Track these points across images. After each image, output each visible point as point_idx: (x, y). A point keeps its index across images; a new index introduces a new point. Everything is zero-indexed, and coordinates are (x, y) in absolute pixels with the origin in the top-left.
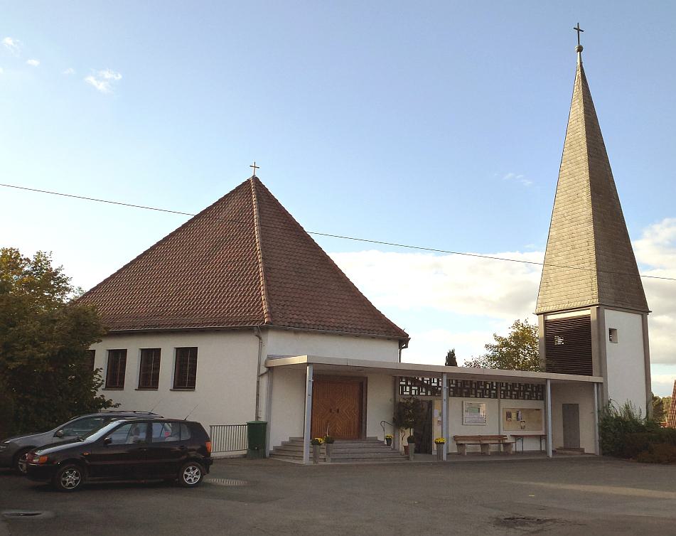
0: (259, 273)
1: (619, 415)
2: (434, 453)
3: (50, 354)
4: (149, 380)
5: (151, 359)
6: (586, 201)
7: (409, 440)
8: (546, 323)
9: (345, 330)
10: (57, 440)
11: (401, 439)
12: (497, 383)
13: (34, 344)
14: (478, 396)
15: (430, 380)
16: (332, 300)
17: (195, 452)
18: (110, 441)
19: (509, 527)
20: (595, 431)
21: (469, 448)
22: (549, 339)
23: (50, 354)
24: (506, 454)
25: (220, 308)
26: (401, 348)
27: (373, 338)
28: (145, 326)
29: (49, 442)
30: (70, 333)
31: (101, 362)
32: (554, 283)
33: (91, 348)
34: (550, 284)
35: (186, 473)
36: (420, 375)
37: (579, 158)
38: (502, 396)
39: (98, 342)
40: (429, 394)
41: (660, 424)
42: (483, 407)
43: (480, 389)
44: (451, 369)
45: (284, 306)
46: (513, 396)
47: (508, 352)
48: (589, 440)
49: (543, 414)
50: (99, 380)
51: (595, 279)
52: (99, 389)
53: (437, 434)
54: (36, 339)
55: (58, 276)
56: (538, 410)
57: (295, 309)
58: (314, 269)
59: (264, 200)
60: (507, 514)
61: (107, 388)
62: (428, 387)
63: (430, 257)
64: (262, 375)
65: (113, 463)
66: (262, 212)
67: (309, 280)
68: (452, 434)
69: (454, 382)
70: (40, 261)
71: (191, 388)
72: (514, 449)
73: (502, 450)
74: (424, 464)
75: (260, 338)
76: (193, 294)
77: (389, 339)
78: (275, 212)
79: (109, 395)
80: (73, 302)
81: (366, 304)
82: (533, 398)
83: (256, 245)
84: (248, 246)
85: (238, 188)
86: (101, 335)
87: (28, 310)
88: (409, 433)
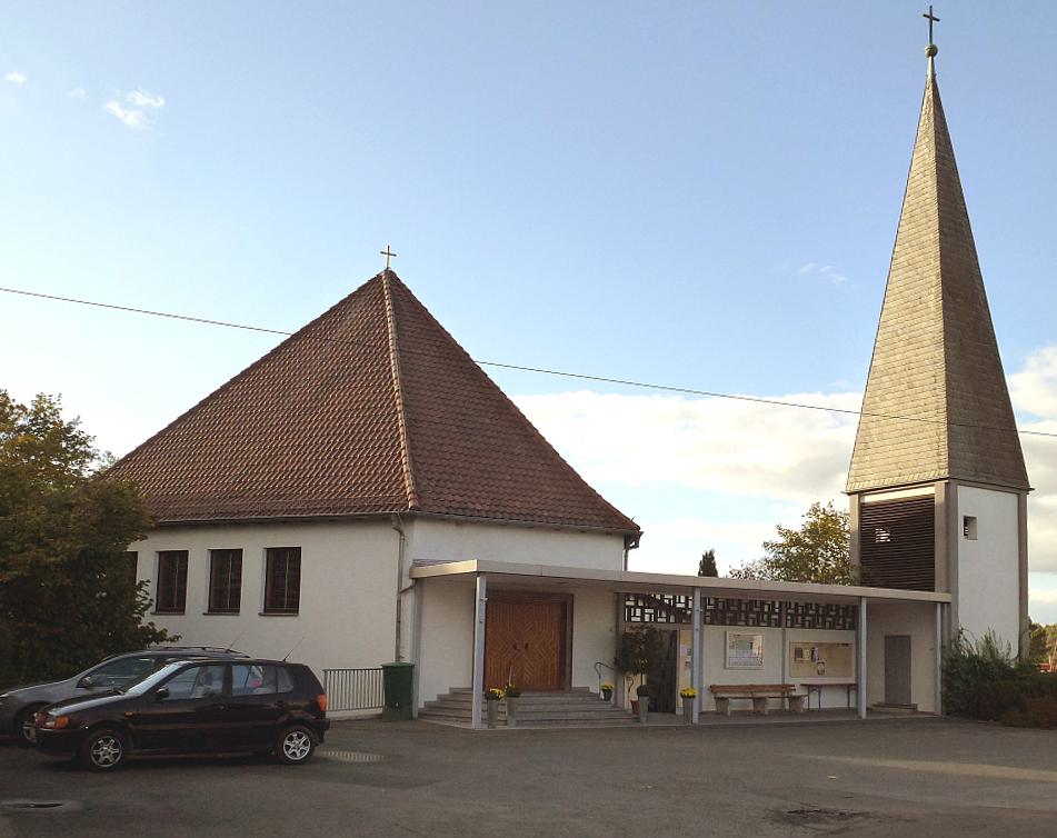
0: (397, 429)
1: (975, 653)
2: (679, 712)
3: (66, 559)
4: (225, 599)
5: (226, 566)
6: (933, 309)
7: (640, 692)
8: (863, 507)
9: (537, 518)
10: (82, 692)
11: (626, 690)
12: (780, 605)
13: (39, 542)
14: (751, 623)
15: (674, 598)
16: (517, 471)
17: (299, 711)
18: (165, 694)
19: (794, 824)
20: (936, 677)
21: (735, 705)
22: (866, 534)
23: (66, 559)
24: (793, 713)
25: (336, 484)
26: (627, 548)
27: (583, 532)
28: (216, 514)
29: (70, 695)
30: (95, 525)
31: (147, 570)
32: (878, 443)
33: (131, 548)
34: (870, 444)
35: (287, 742)
36: (657, 591)
37: (925, 238)
38: (789, 623)
39: (142, 539)
40: (672, 620)
41: (1039, 666)
42: (758, 641)
43: (754, 613)
44: (708, 582)
45: (438, 480)
46: (807, 623)
47: (798, 555)
48: (925, 691)
49: (854, 651)
50: (146, 599)
51: (944, 437)
52: (146, 613)
53: (684, 682)
54: (42, 534)
55: (73, 433)
56: (847, 645)
57: (457, 485)
58: (488, 421)
59: (405, 308)
60: (794, 805)
61: (160, 610)
62: (671, 609)
63: (675, 403)
64: (405, 590)
65: (171, 727)
66: (402, 330)
67: (480, 440)
68: (707, 683)
69: (712, 602)
70: (42, 410)
71: (292, 612)
72: (805, 706)
73: (787, 707)
74: (663, 729)
75: (401, 533)
76: (293, 462)
77: (608, 534)
78: (422, 329)
79: (163, 622)
80: (99, 476)
81: (571, 478)
82: (762, 624)
83: (392, 383)
84: (380, 385)
85: (361, 289)
86: (144, 528)
87: (27, 489)
88: (639, 680)
